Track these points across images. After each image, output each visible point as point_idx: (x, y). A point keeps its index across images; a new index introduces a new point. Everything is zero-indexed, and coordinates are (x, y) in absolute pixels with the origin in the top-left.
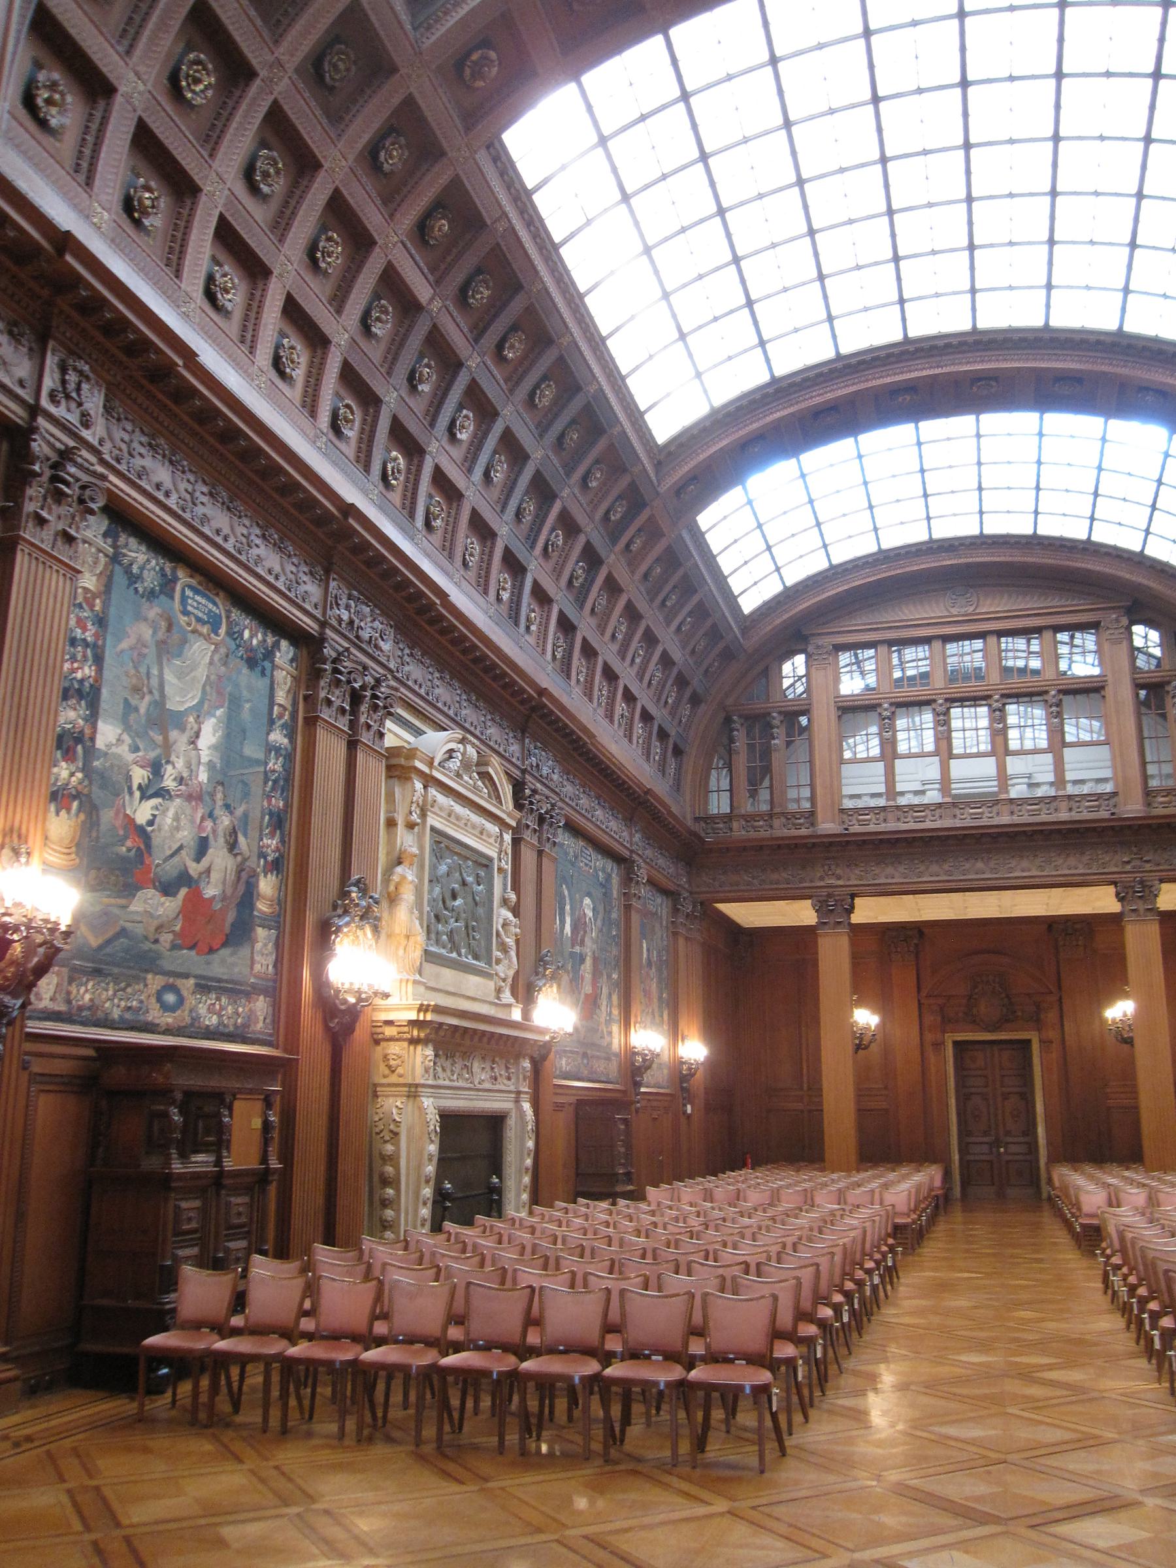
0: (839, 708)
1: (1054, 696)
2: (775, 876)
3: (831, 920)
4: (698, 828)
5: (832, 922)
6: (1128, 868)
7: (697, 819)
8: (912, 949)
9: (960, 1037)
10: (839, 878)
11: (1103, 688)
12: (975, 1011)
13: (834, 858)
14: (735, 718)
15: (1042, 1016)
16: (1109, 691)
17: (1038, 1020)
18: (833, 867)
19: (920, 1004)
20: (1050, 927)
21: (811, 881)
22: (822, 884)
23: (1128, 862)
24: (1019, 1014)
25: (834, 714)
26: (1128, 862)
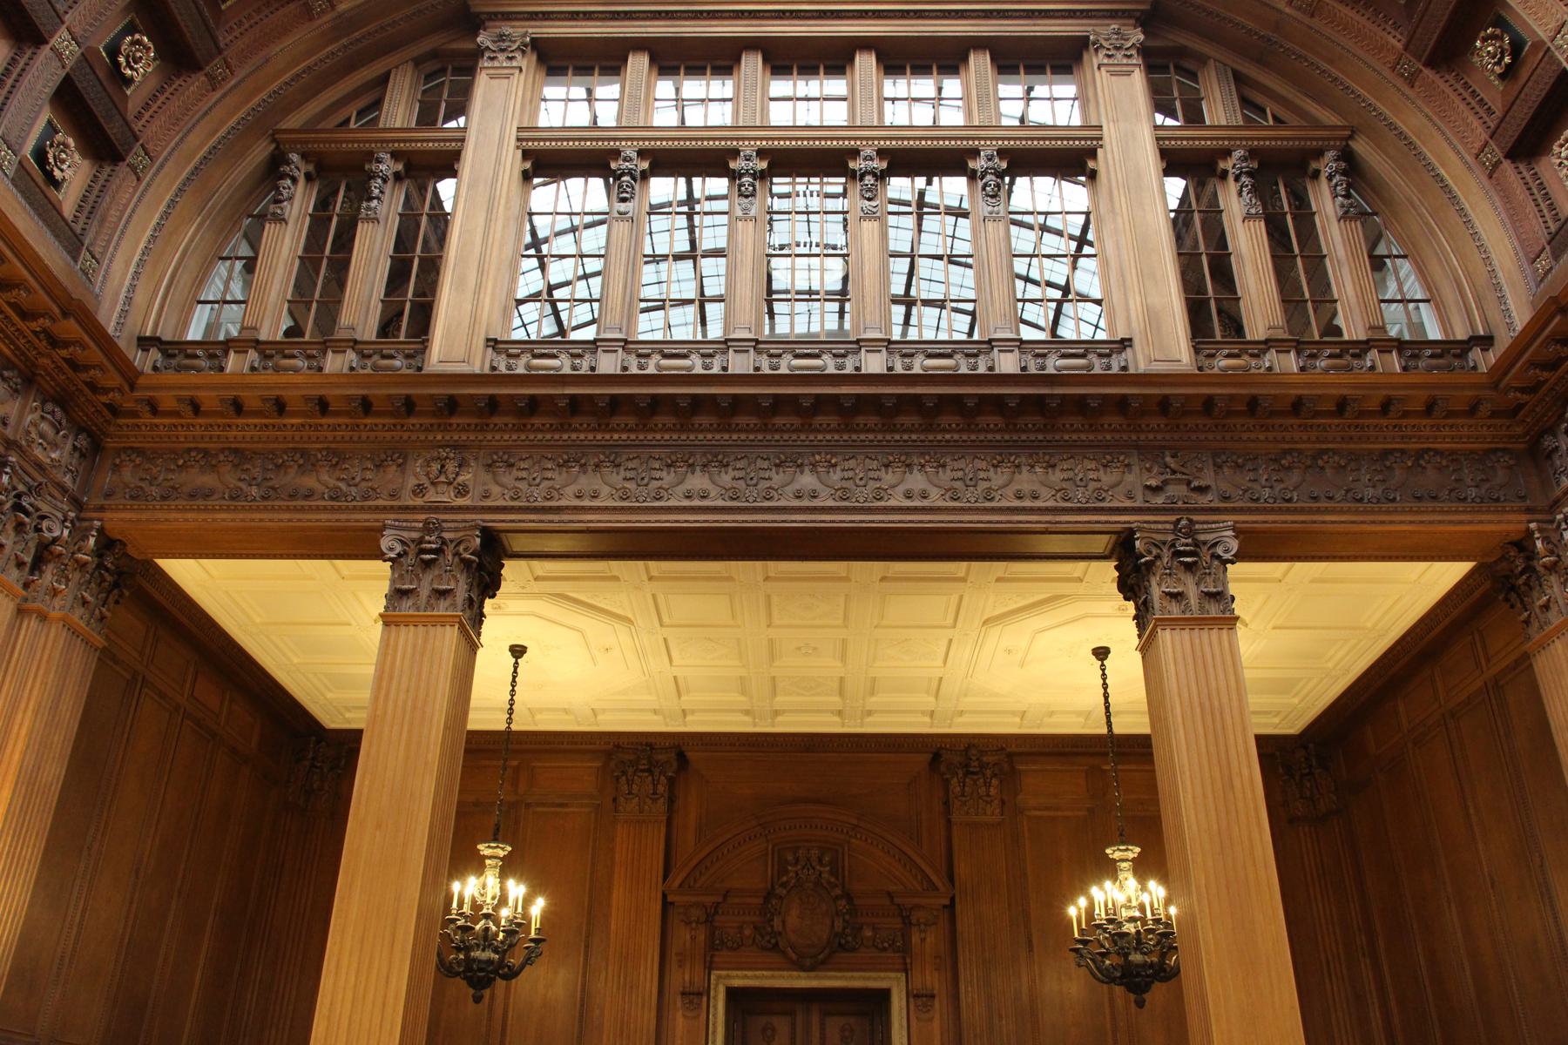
0: (526, 154)
1: (990, 159)
2: (310, 482)
3: (426, 584)
4: (144, 361)
5: (425, 592)
6: (1159, 500)
7: (145, 343)
8: (661, 789)
9: (741, 980)
10: (462, 491)
11: (1092, 153)
12: (777, 922)
13: (455, 446)
14: (295, 157)
15: (915, 939)
16: (1105, 162)
17: (906, 950)
18: (451, 467)
19: (666, 905)
20: (936, 757)
21: (392, 496)
22: (419, 502)
23: (1156, 490)
24: (868, 933)
25: (513, 162)
26: (1156, 490)
